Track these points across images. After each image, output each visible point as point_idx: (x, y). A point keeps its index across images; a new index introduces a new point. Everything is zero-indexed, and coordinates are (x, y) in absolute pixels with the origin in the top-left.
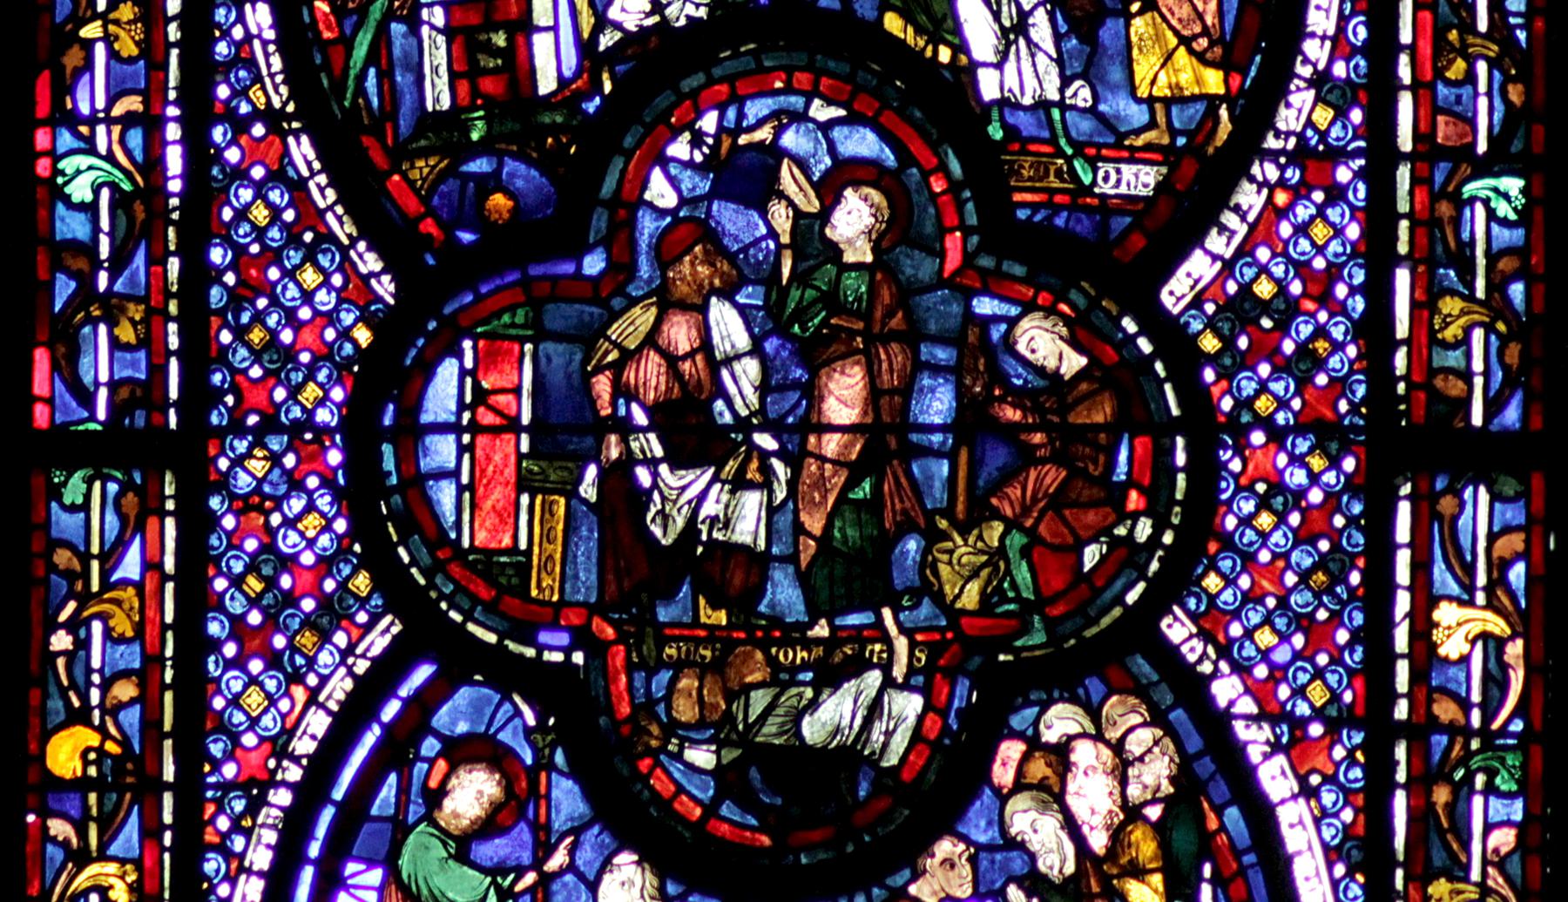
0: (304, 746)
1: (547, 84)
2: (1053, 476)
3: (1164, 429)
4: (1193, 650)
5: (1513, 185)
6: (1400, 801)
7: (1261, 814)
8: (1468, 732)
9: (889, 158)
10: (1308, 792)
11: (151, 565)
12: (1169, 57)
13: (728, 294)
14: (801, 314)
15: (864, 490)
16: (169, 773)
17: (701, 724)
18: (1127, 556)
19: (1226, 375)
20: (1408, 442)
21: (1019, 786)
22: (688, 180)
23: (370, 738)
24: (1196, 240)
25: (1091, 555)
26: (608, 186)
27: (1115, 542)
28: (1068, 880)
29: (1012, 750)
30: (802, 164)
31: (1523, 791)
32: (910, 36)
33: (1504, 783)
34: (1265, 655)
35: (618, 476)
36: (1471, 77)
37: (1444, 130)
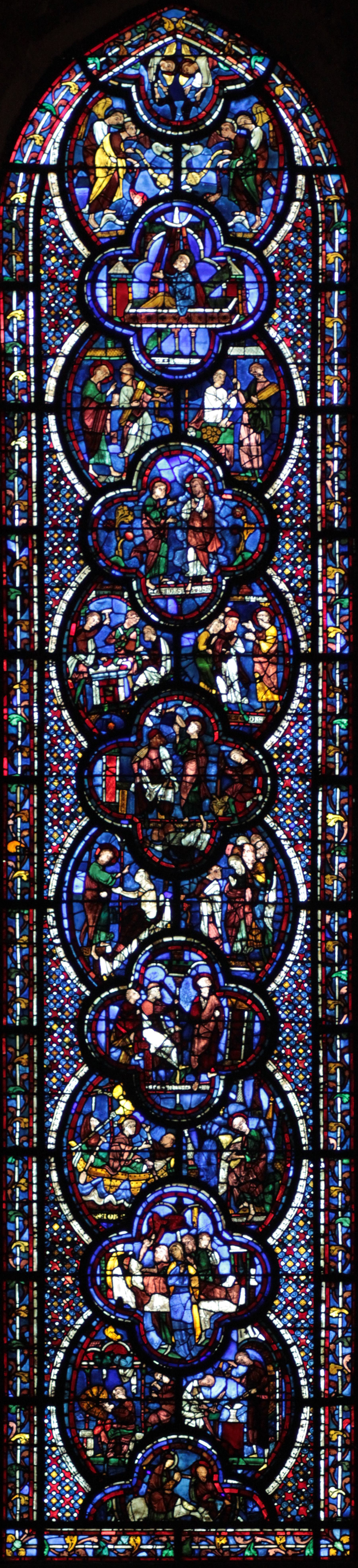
0: (67, 845)
1: (122, 698)
2: (239, 786)
3: (265, 776)
4: (272, 825)
5: (345, 721)
6: (319, 858)
7: (287, 860)
8: (334, 842)
9: (201, 715)
10: (298, 856)
11: (31, 805)
12: (265, 693)
13: (164, 745)
14: (181, 750)
15: (196, 789)
16: (36, 851)
17: (159, 841)
18: (256, 804)
19: (279, 763)
20: (321, 778)
21: (232, 854)
22: (155, 720)
23: (83, 844)
24: (272, 733)
25: (248, 804)
26: (137, 721)
27: (254, 801)
28: (243, 875)
29: (230, 847)
30: (181, 716)
31: (347, 855)
32: (206, 687)
33: (343, 853)
34: (288, 826)
35: (139, 786)
36: (335, 697)
37: (329, 709)
